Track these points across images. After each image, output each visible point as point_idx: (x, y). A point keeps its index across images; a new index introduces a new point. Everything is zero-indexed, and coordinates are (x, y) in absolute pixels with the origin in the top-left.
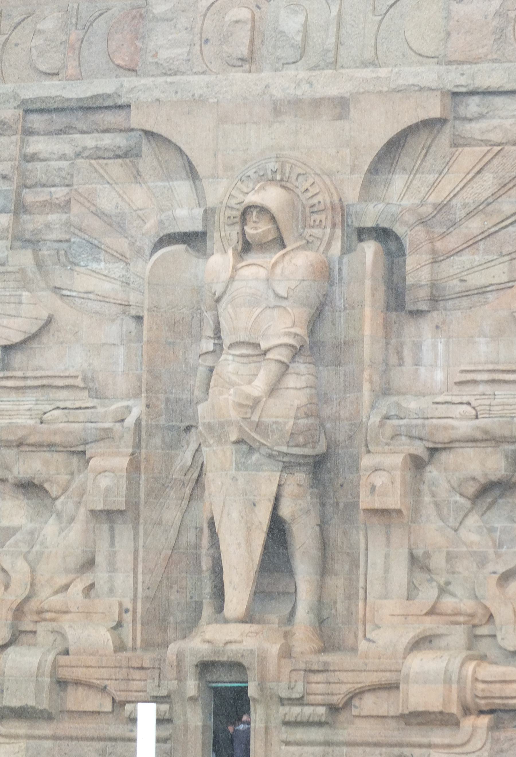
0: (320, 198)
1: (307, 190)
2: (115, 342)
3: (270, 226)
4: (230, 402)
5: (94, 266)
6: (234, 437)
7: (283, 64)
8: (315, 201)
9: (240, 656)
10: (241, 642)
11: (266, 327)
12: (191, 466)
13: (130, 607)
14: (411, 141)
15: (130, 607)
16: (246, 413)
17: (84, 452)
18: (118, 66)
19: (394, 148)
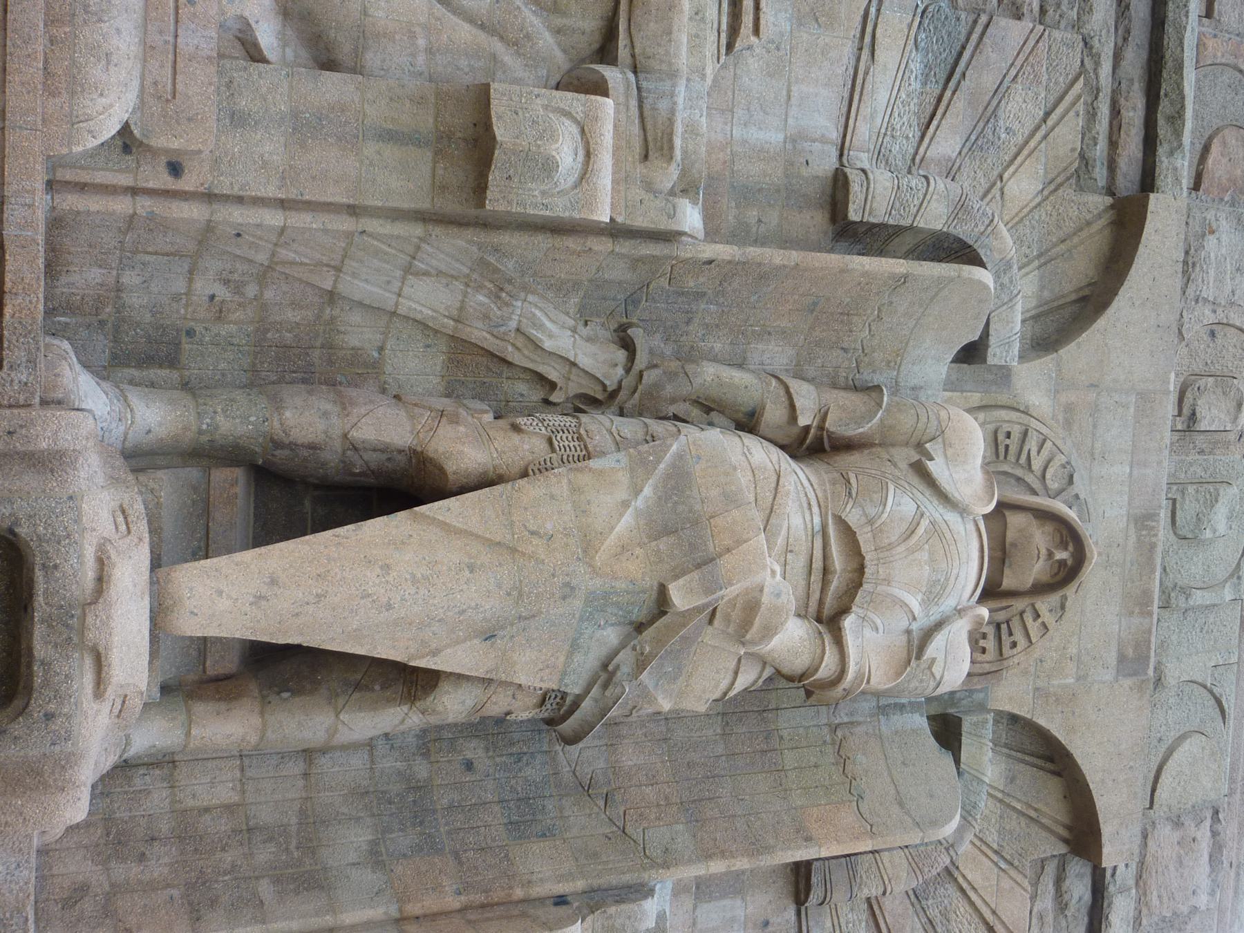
0: (1022, 643)
1: (1037, 616)
2: (790, 121)
3: (1029, 582)
4: (757, 579)
5: (916, 66)
6: (680, 598)
7: (1174, 501)
8: (1019, 636)
9: (52, 707)
10: (99, 693)
11: (878, 622)
12: (537, 347)
13: (188, 183)
14: (1053, 787)
15: (188, 183)
16: (727, 619)
17: (612, 61)
18: (1206, 149)
19: (1050, 757)
